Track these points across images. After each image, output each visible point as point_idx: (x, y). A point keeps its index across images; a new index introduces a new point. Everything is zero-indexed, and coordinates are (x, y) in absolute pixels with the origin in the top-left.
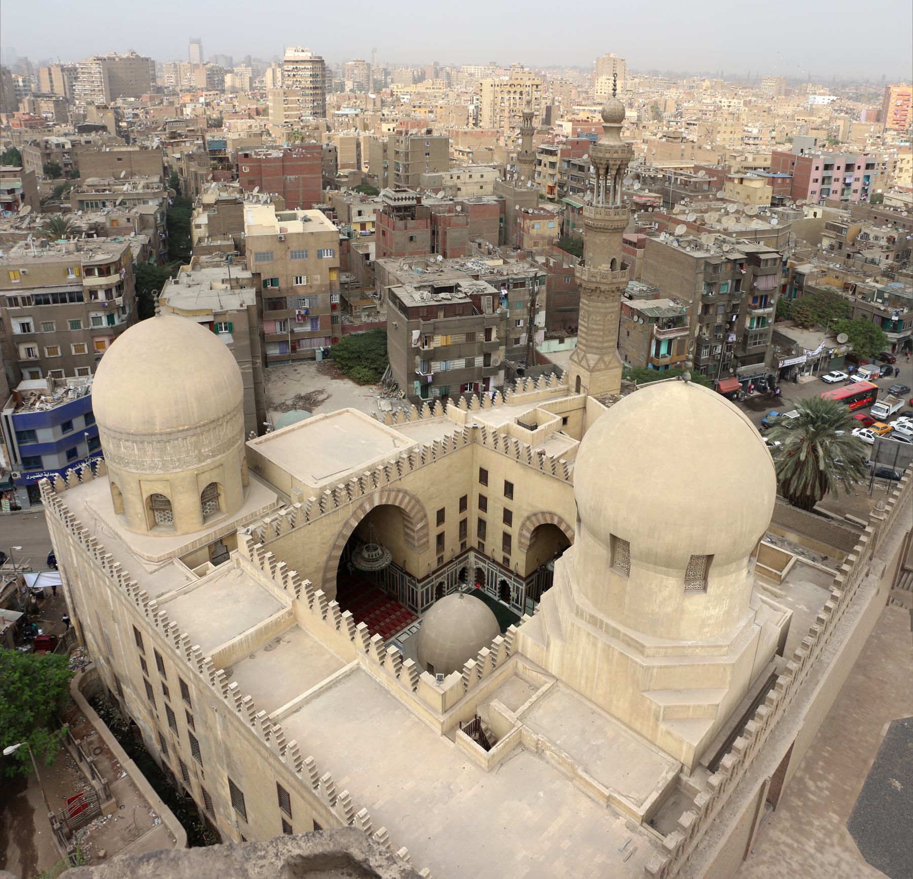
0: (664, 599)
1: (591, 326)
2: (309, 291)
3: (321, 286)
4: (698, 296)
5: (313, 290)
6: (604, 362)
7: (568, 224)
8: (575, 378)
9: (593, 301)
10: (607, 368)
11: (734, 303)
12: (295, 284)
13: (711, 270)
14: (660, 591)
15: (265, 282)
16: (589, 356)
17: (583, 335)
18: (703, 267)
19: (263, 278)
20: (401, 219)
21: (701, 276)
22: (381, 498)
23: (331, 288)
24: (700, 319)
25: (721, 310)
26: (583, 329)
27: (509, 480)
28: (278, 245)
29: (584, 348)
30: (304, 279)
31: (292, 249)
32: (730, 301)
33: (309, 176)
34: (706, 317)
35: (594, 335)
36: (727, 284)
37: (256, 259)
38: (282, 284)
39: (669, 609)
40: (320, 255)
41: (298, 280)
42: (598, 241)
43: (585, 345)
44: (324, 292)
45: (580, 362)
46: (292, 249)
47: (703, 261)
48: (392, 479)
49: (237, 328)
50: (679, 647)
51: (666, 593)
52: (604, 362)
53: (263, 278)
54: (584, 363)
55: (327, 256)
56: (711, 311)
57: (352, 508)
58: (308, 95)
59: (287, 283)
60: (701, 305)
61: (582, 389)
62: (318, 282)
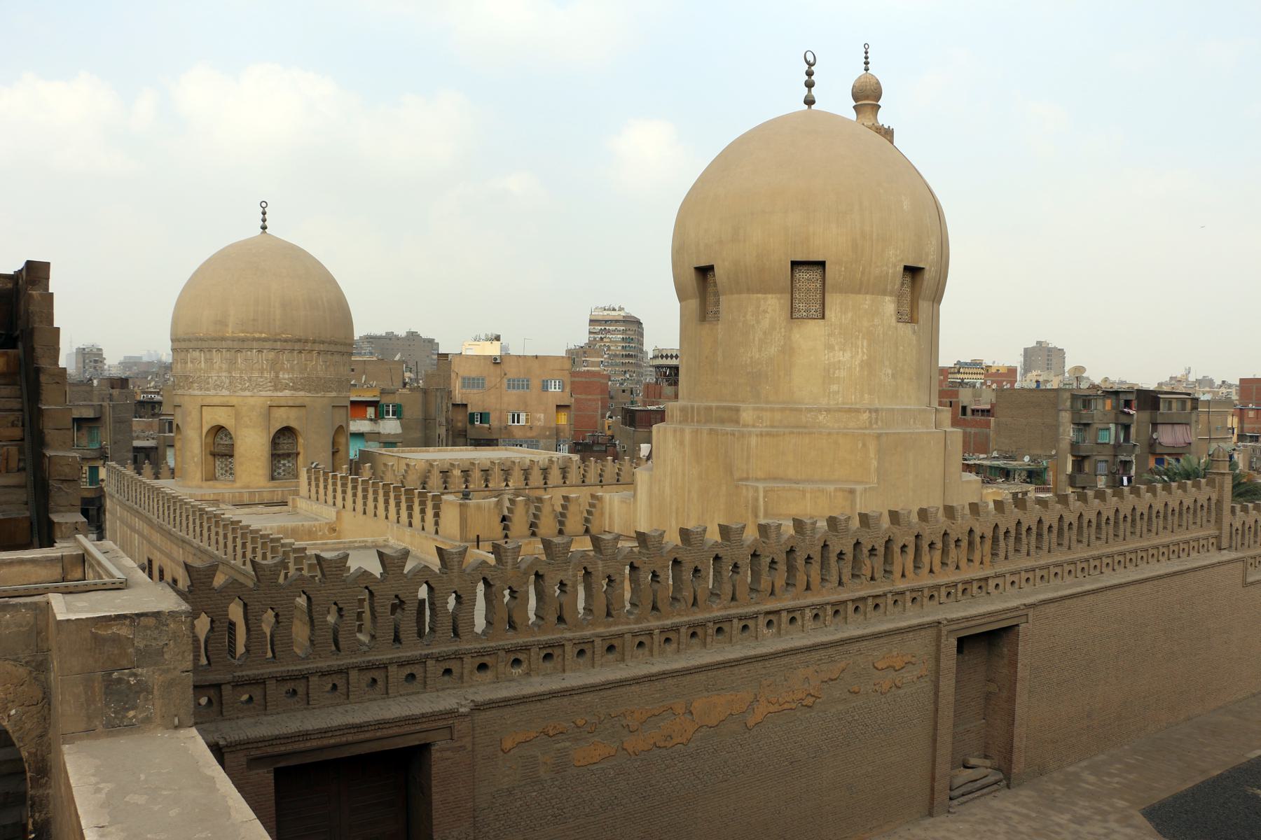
0: (765, 333)
2: (529, 434)
3: (544, 428)
4: (1065, 445)
5: (533, 434)
11: (1123, 458)
12: (510, 423)
13: (1079, 405)
14: (758, 322)
15: (472, 415)
18: (1068, 404)
19: (470, 410)
20: (670, 385)
21: (1066, 417)
23: (557, 434)
24: (1072, 481)
25: (1102, 468)
28: (492, 367)
30: (523, 417)
31: (509, 376)
32: (1115, 456)
33: (583, 397)
34: (1080, 479)
36: (1109, 429)
37: (463, 386)
38: (494, 422)
39: (773, 350)
40: (545, 387)
41: (515, 418)
44: (549, 437)
46: (509, 376)
47: (1067, 395)
49: (407, 413)
50: (792, 410)
51: (766, 323)
53: (470, 410)
55: (554, 388)
56: (1087, 467)
58: (617, 365)
59: (500, 420)
60: (1070, 460)
62: (541, 423)
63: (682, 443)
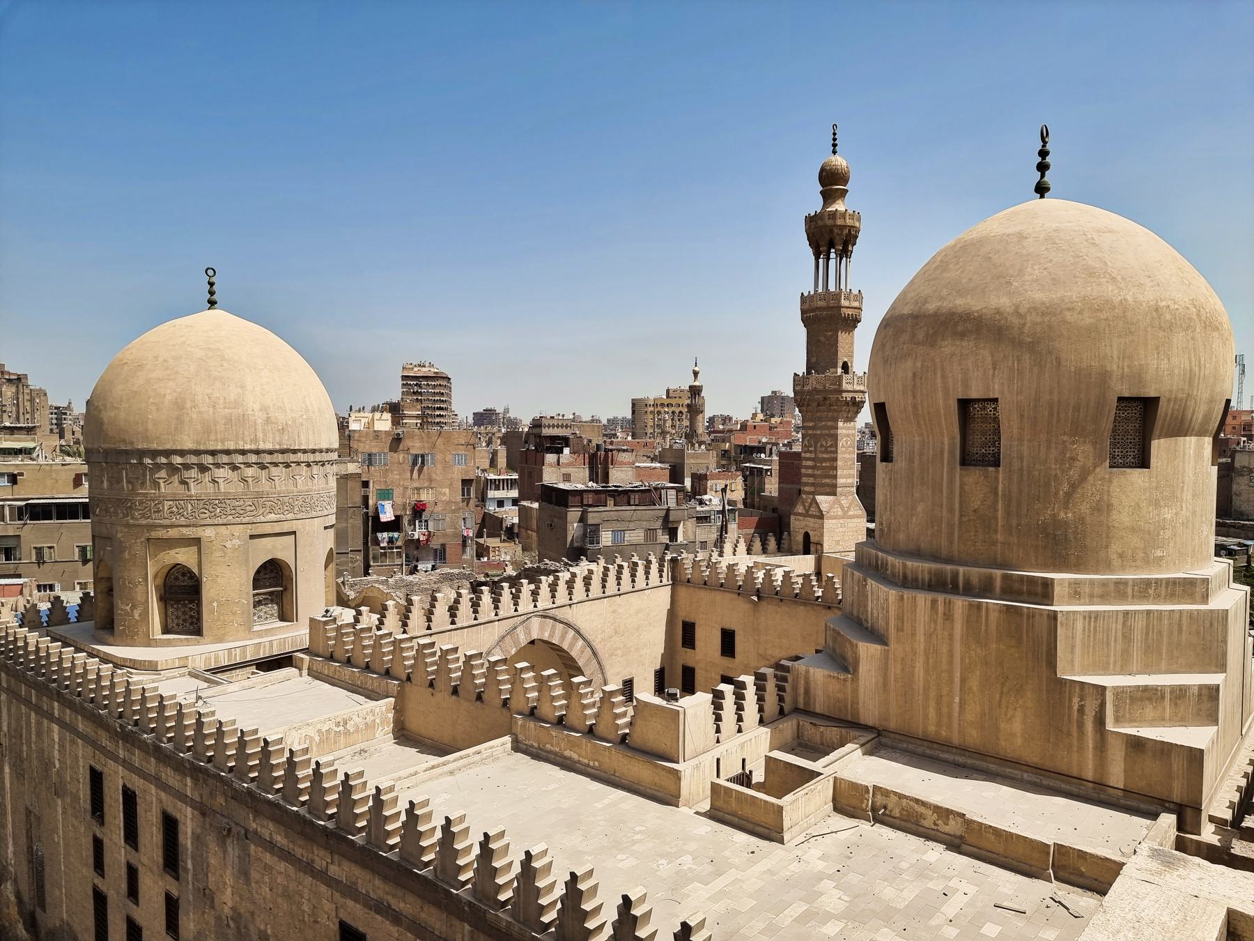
1: (820, 455)
6: (842, 507)
7: (752, 494)
8: (800, 538)
9: (820, 419)
10: (845, 516)
16: (819, 498)
17: (810, 471)
22: (542, 629)
26: (810, 463)
27: (727, 626)
29: (812, 489)
35: (824, 468)
42: (822, 339)
43: (813, 485)
45: (807, 511)
48: (559, 602)
52: (842, 507)
54: (813, 511)
57: (498, 629)
61: (812, 548)
63: (948, 616)
